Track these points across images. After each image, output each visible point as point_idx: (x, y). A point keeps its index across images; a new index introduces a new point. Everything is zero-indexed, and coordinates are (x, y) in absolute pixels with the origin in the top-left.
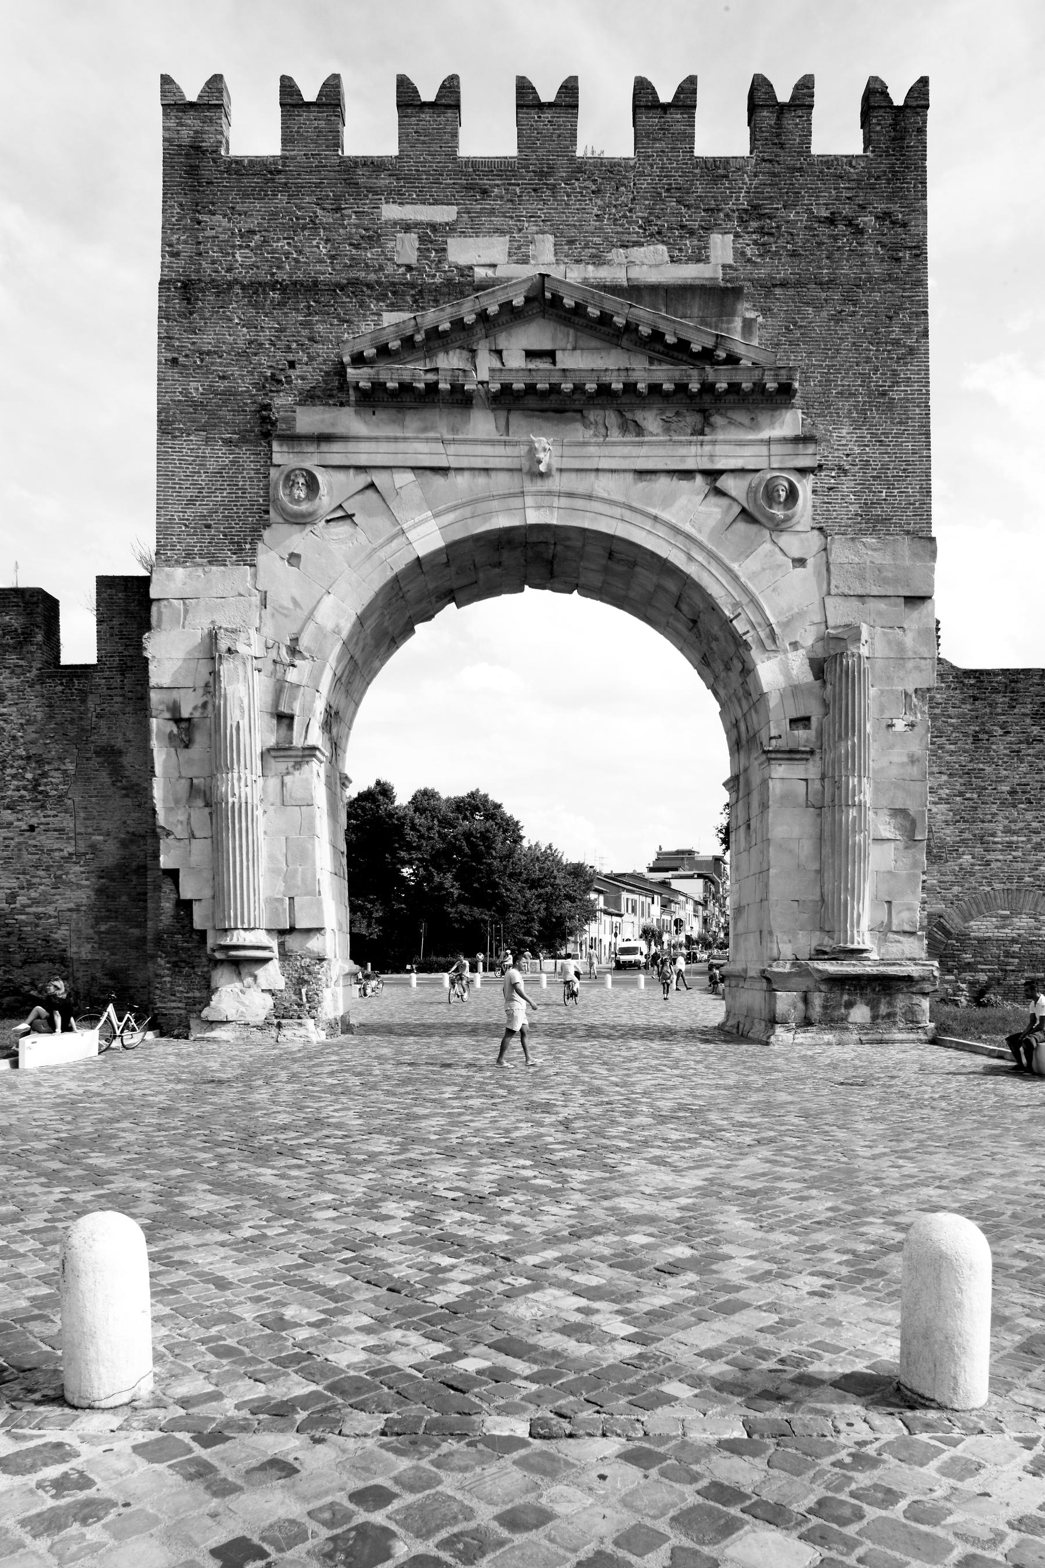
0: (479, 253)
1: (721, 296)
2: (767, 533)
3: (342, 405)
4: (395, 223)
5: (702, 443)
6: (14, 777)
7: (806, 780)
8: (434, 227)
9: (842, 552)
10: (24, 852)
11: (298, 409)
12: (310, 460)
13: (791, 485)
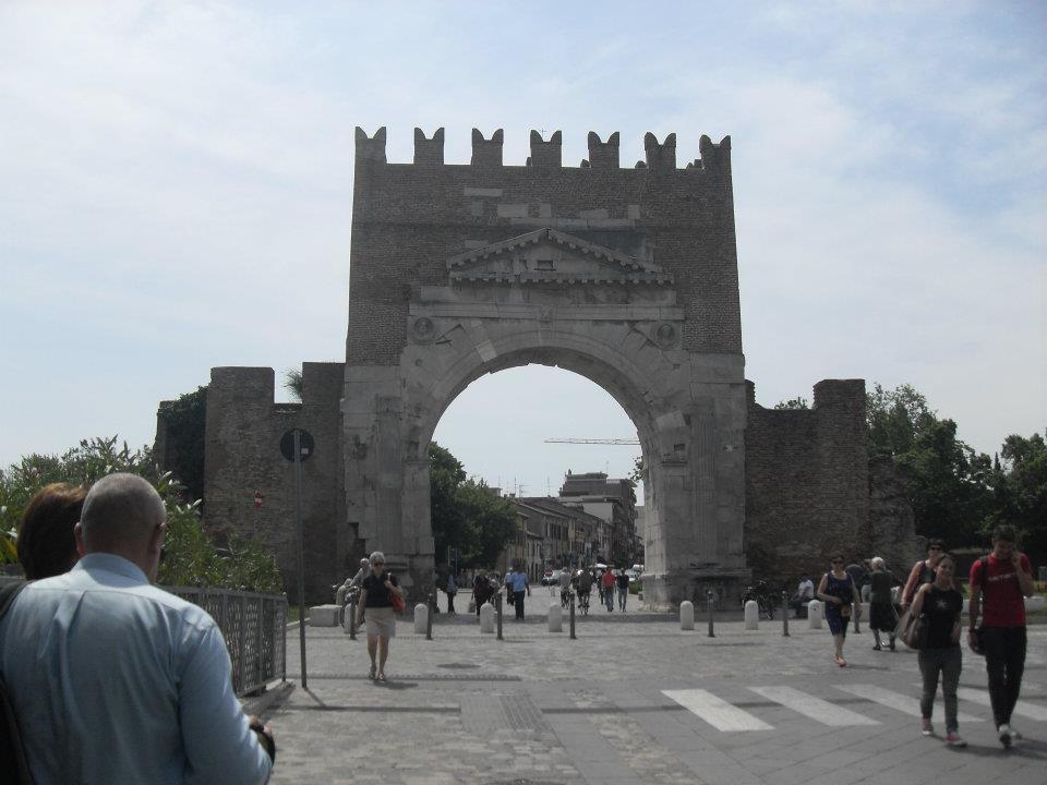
0: (515, 212)
1: (630, 237)
2: (660, 351)
3: (445, 285)
5: (627, 308)
6: (253, 469)
8: (491, 198)
12: (427, 313)
13: (672, 329)
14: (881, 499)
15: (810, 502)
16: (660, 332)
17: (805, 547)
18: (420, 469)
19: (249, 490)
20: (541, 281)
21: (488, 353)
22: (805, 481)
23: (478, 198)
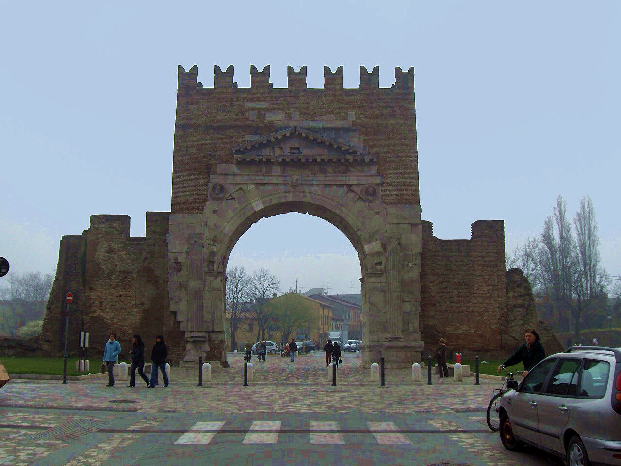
0: (277, 118)
4: (249, 108)
7: (381, 283)
9: (392, 210)
10: (117, 304)
11: (218, 165)
13: (374, 189)
14: (514, 297)
15: (468, 298)
16: (367, 192)
17: (465, 327)
18: (216, 278)
19: (113, 291)
20: (292, 160)
21: (258, 206)
22: (465, 285)
23: (253, 109)
